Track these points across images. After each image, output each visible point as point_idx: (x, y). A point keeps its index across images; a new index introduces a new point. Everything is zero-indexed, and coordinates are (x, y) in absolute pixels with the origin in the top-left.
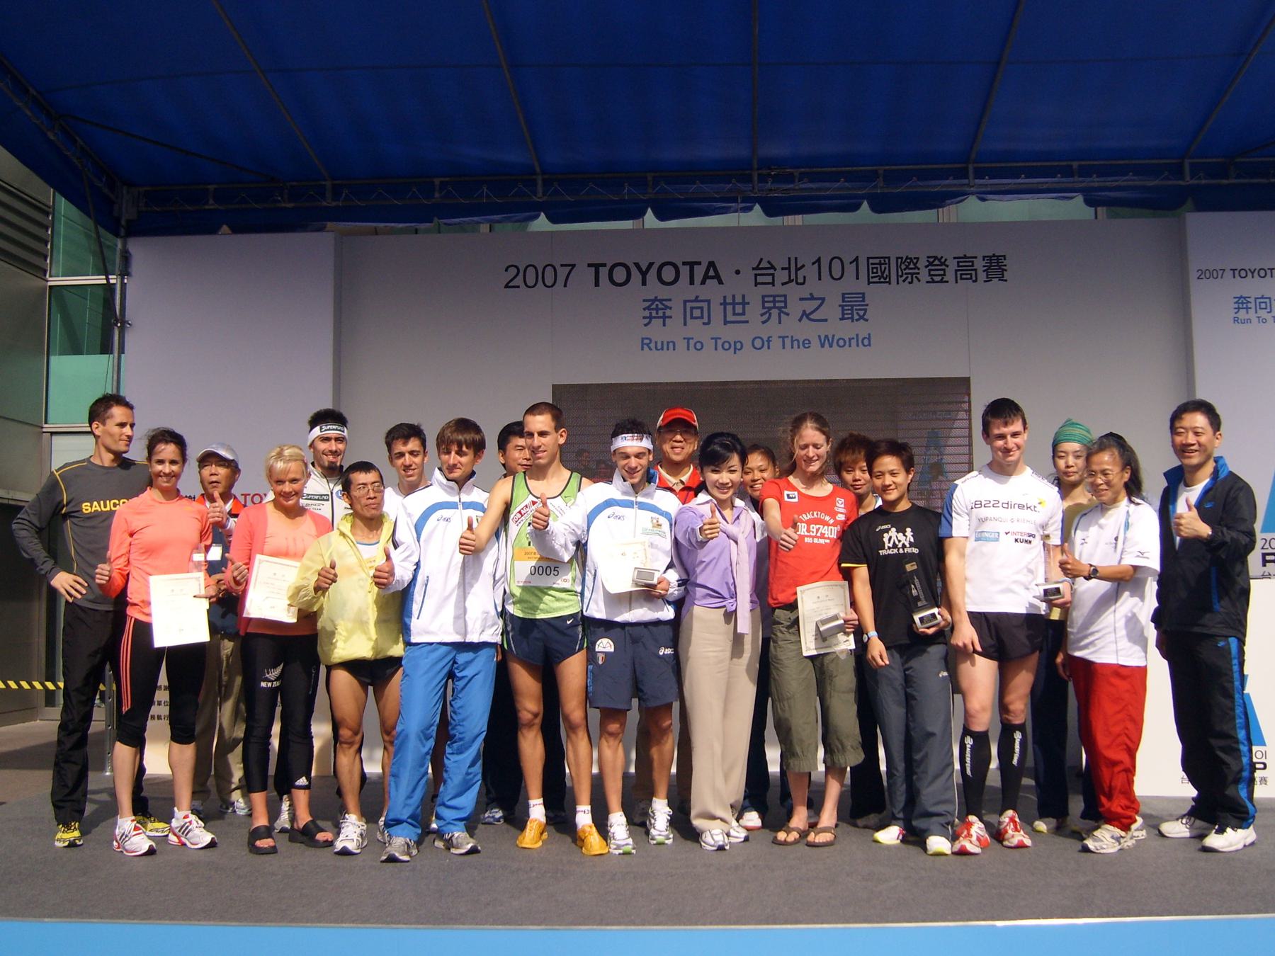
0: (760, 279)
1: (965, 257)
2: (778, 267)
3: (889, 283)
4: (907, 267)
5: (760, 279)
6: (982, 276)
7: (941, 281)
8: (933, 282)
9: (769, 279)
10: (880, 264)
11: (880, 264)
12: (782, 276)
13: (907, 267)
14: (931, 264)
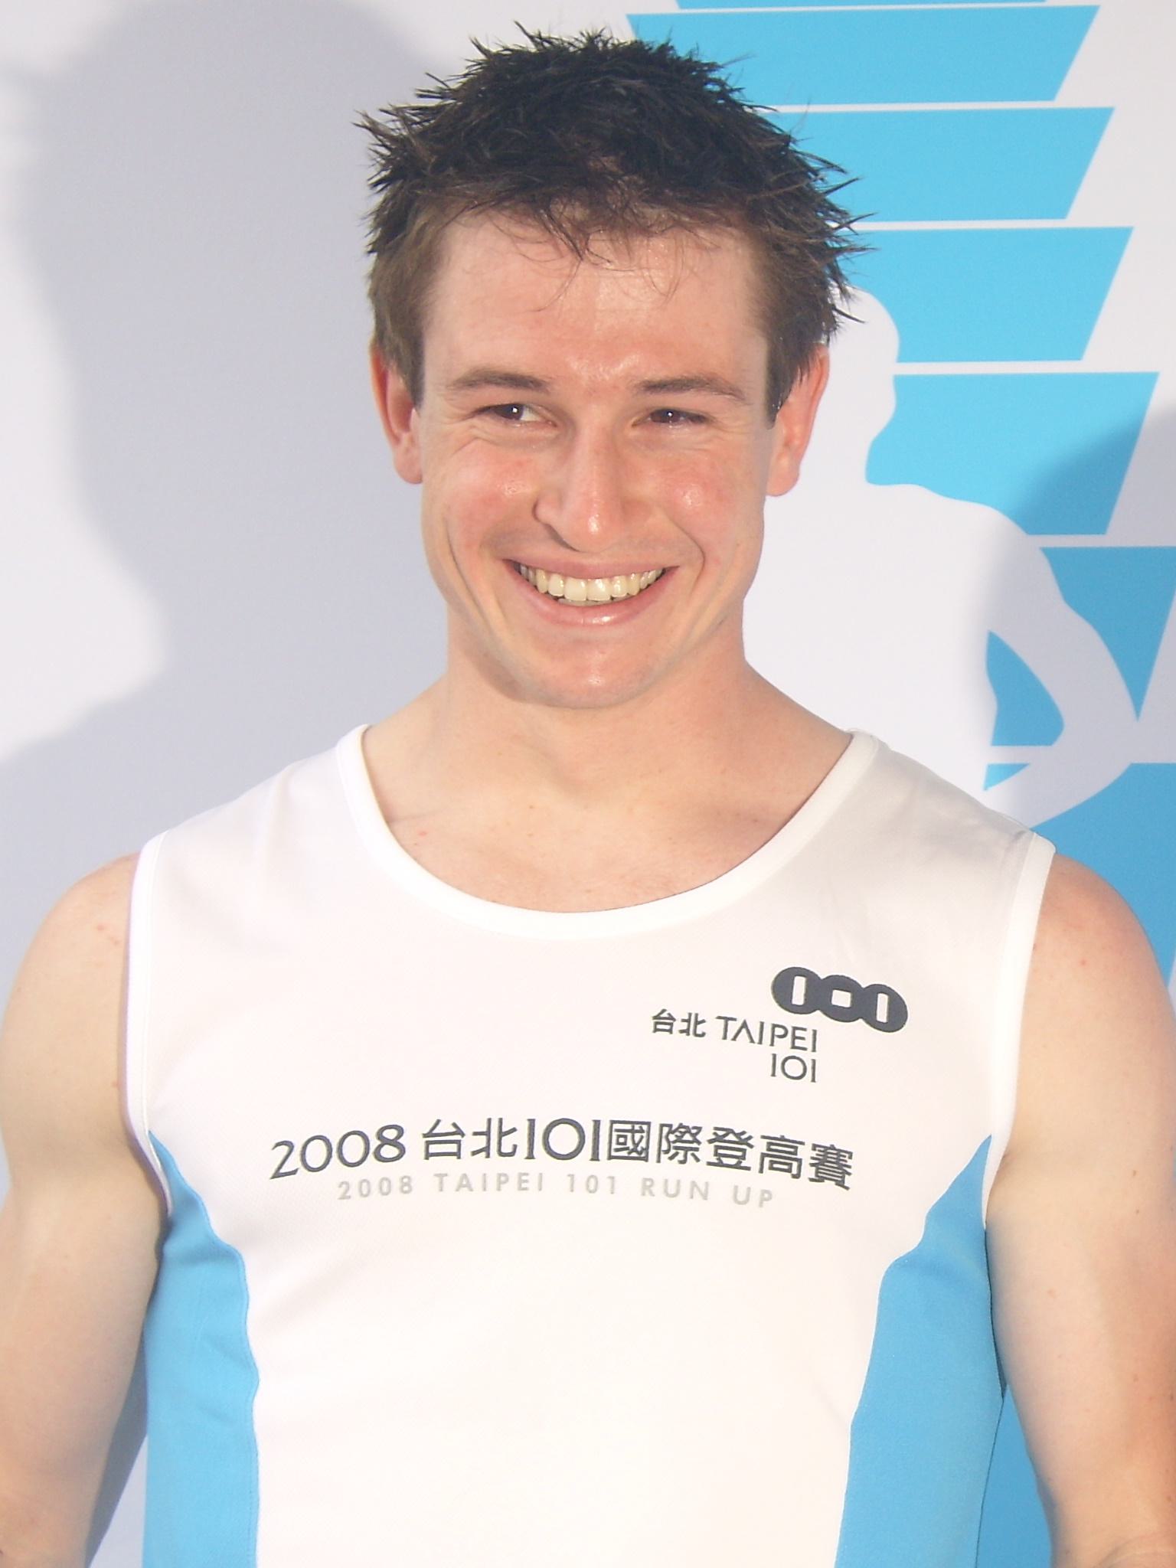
0: (433, 1149)
1: (782, 1139)
2: (468, 1130)
3: (646, 1159)
4: (679, 1140)
5: (433, 1149)
6: (808, 1171)
7: (737, 1166)
8: (720, 1164)
9: (453, 1148)
10: (633, 1131)
11: (633, 1131)
12: (471, 1143)
13: (679, 1140)
14: (718, 1138)
